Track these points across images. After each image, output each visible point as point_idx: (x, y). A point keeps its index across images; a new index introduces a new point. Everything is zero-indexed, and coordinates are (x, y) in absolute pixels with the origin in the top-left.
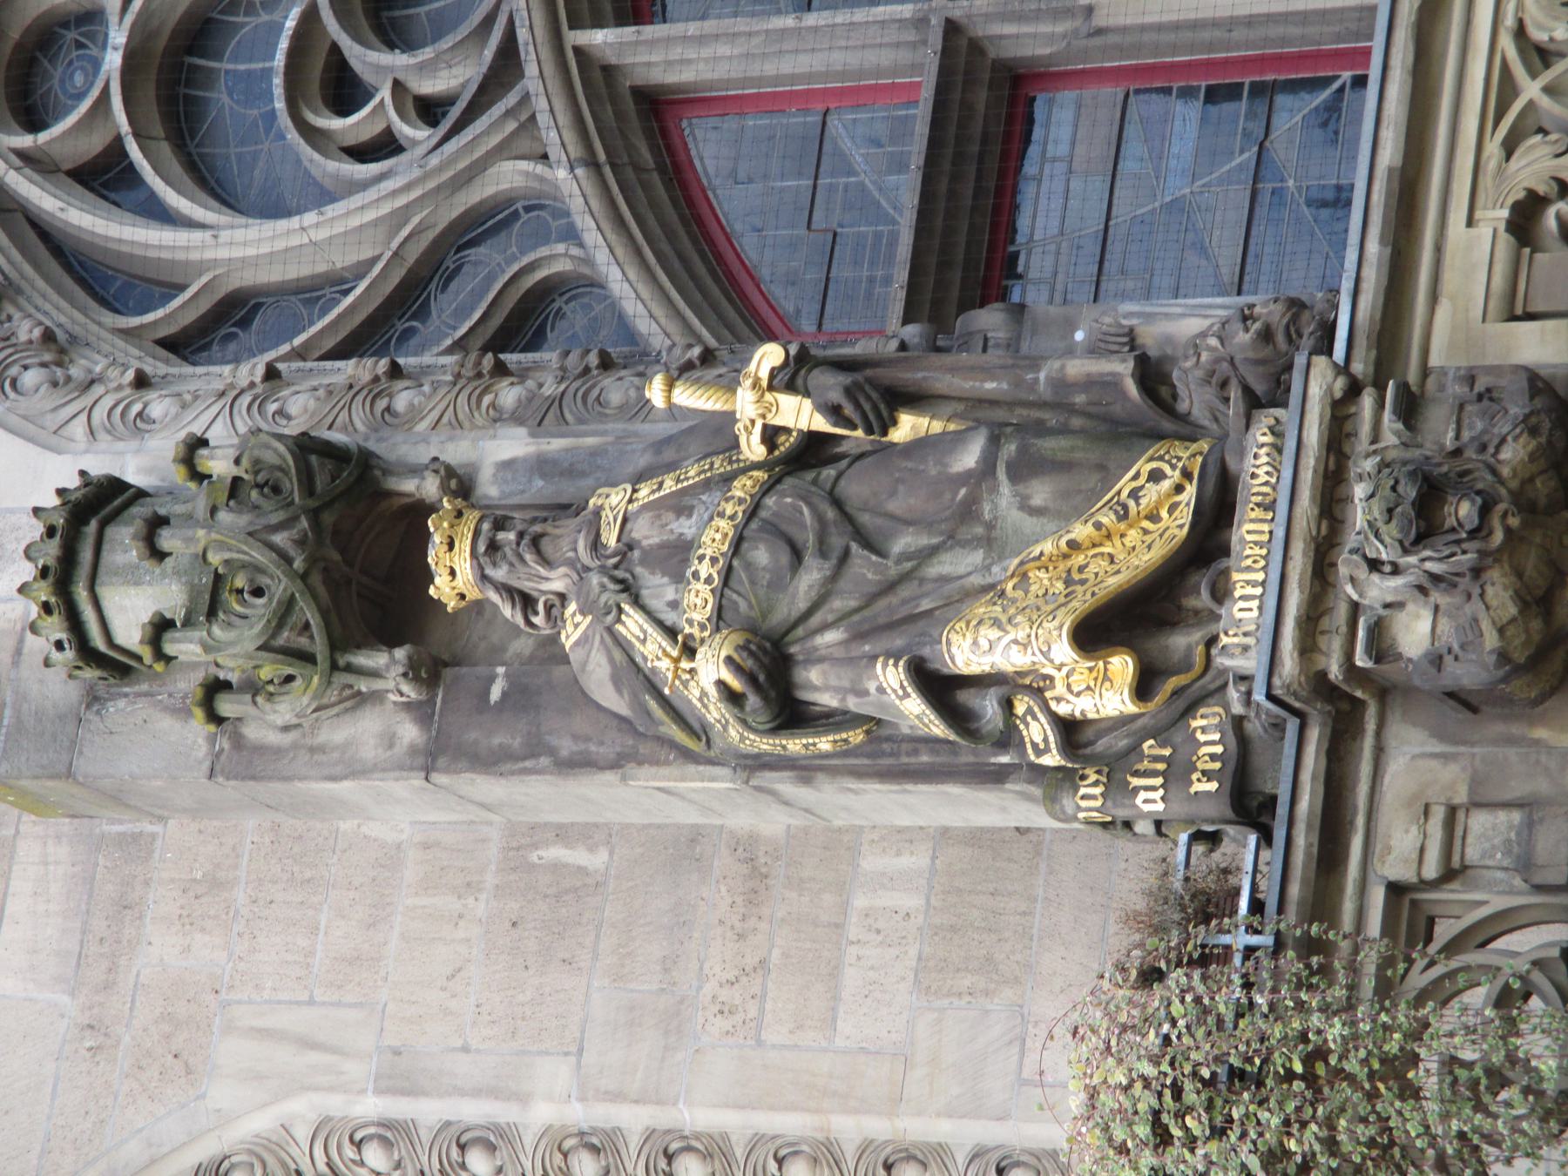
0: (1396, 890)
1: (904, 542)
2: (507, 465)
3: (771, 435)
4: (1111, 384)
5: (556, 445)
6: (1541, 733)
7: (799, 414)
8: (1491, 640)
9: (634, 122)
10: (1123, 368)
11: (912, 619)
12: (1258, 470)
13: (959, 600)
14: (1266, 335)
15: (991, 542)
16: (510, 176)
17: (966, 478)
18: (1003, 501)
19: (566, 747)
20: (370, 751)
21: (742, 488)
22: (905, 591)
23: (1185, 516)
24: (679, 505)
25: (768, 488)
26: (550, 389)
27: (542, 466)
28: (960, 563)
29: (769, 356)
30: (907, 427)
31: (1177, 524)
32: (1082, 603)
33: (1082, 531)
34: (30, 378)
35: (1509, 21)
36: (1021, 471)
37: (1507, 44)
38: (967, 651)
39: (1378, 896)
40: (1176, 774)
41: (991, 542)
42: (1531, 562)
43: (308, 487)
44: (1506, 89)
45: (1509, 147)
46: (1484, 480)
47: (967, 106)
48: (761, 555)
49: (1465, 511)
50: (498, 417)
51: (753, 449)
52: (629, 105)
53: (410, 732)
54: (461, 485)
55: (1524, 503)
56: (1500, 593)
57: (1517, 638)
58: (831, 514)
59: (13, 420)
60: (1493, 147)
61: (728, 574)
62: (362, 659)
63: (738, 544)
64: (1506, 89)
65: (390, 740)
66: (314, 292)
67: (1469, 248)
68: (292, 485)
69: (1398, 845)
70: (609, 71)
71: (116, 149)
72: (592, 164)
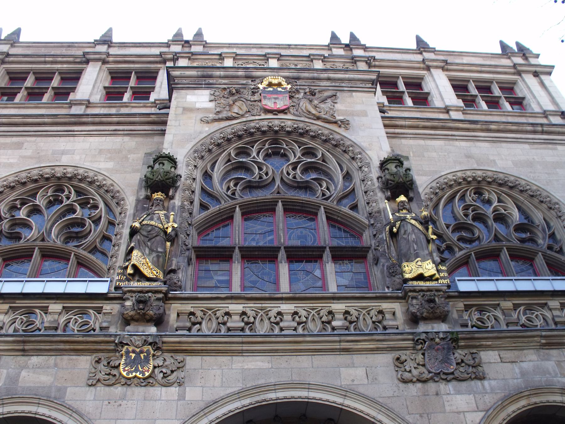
0: (102, 307)
1: (149, 243)
2: (175, 203)
3: (167, 228)
4: (171, 265)
5: (177, 208)
6: (120, 322)
7: (169, 230)
8: (125, 312)
9: (229, 215)
10: (173, 267)
11: (140, 246)
12: (155, 284)
13: (140, 249)
14: (175, 283)
15: (150, 254)
16: (223, 202)
17: (157, 249)
18: (154, 255)
19: (136, 214)
20: (140, 193)
21: (160, 225)
22: (144, 245)
23: (152, 276)
24: (159, 218)
25: (160, 228)
26: (186, 207)
27: (174, 207)
28: (147, 251)
29: (176, 226)
30: (168, 244)
31: (150, 275)
32: (138, 265)
33: (150, 264)
34: (196, 155)
35: (220, 308)
36: (158, 257)
37: (217, 309)
38: (135, 253)
39: (101, 305)
40: (120, 281)
41: (150, 254)
42: (137, 316)
43: (167, 179)
44: (210, 309)
45: (202, 311)
46: (146, 309)
47: (225, 251)
48: (150, 228)
49: (141, 306)
50: (182, 202)
51: (166, 226)
52: (231, 214)
53: (142, 197)
54: (172, 198)
55: (144, 314)
56: (132, 313)
57: (127, 316)
58: (154, 235)
59: (189, 153)
60: (202, 309)
61: (148, 225)
62: (149, 190)
63: (152, 225)
64: (210, 309)
65: (141, 196)
66: (212, 186)
67: (188, 307)
68: (167, 177)
69: (108, 307)
70: (234, 211)
71: (231, 161)
72: (220, 210)
